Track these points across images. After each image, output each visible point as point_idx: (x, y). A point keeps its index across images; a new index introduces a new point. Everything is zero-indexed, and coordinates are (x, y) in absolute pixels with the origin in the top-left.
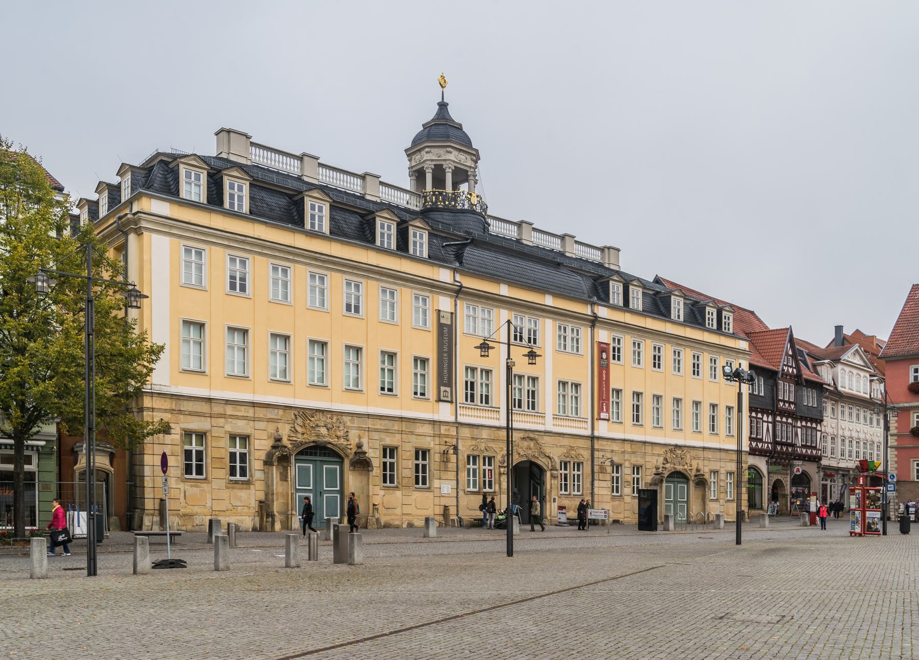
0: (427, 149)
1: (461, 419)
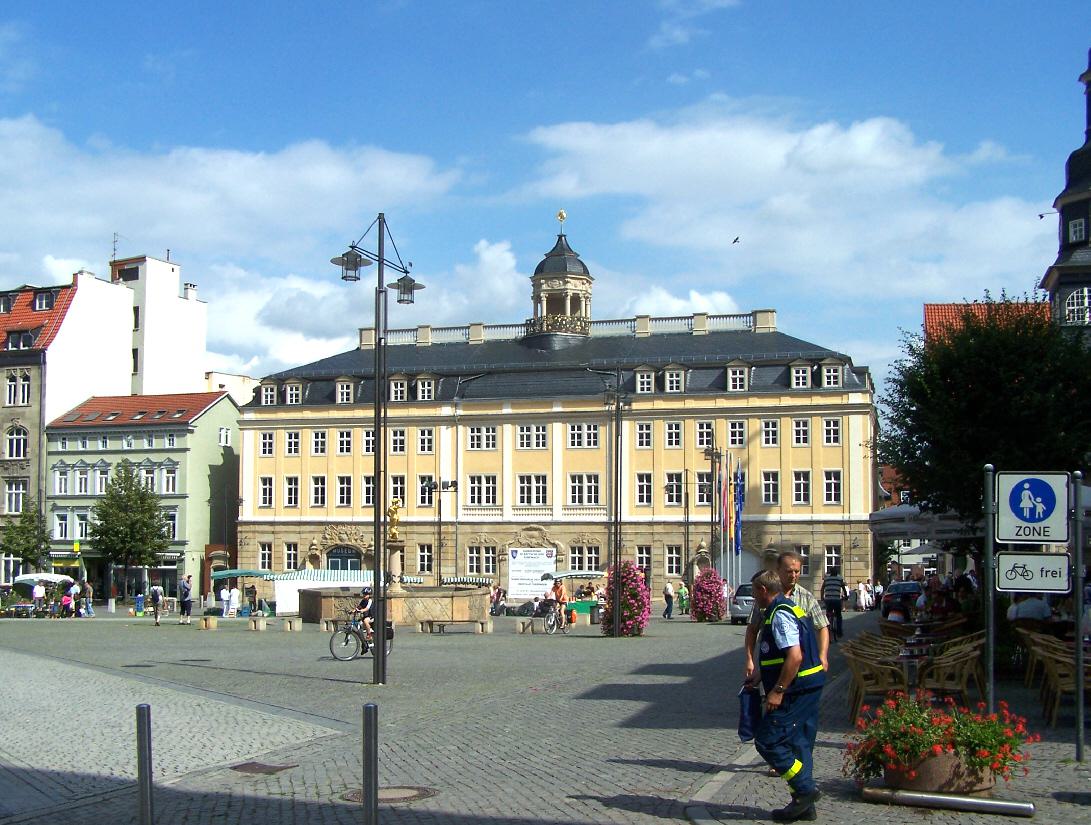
1: (462, 519)
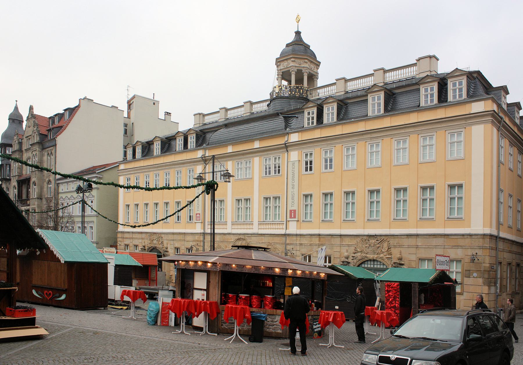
0: (307, 61)
